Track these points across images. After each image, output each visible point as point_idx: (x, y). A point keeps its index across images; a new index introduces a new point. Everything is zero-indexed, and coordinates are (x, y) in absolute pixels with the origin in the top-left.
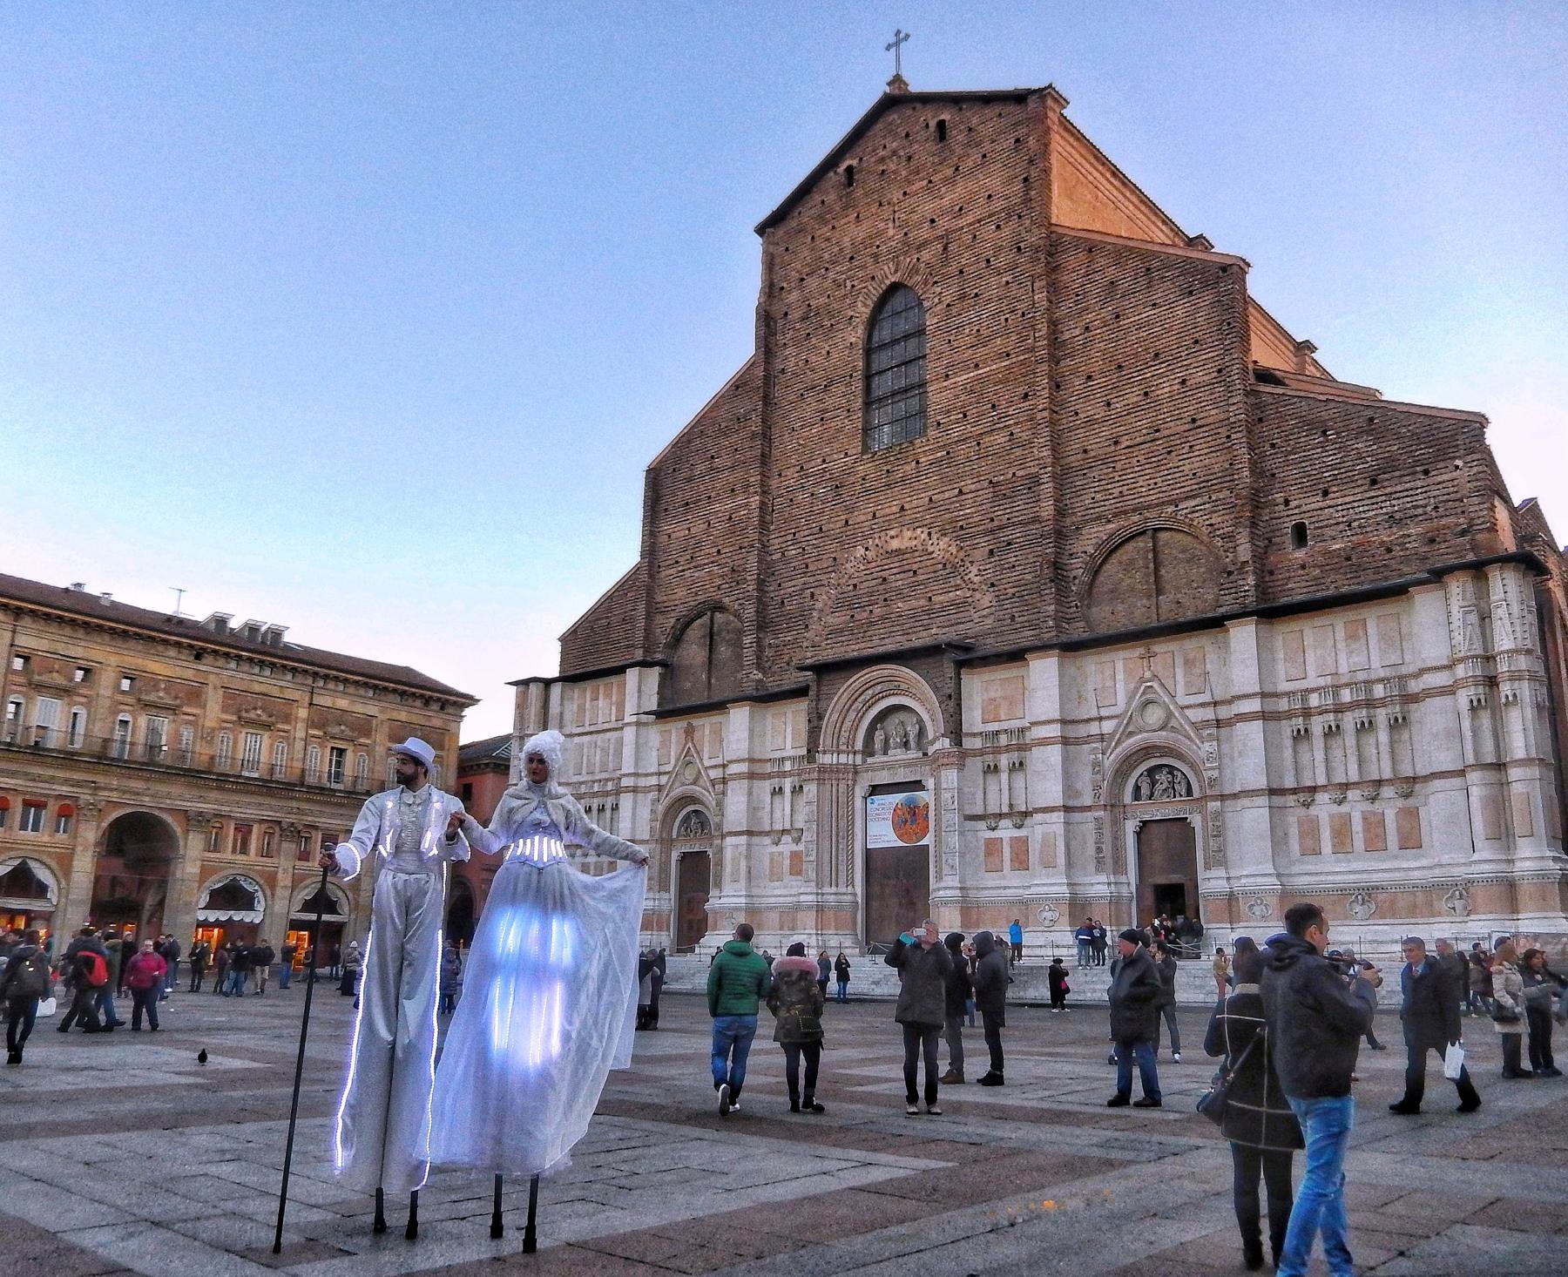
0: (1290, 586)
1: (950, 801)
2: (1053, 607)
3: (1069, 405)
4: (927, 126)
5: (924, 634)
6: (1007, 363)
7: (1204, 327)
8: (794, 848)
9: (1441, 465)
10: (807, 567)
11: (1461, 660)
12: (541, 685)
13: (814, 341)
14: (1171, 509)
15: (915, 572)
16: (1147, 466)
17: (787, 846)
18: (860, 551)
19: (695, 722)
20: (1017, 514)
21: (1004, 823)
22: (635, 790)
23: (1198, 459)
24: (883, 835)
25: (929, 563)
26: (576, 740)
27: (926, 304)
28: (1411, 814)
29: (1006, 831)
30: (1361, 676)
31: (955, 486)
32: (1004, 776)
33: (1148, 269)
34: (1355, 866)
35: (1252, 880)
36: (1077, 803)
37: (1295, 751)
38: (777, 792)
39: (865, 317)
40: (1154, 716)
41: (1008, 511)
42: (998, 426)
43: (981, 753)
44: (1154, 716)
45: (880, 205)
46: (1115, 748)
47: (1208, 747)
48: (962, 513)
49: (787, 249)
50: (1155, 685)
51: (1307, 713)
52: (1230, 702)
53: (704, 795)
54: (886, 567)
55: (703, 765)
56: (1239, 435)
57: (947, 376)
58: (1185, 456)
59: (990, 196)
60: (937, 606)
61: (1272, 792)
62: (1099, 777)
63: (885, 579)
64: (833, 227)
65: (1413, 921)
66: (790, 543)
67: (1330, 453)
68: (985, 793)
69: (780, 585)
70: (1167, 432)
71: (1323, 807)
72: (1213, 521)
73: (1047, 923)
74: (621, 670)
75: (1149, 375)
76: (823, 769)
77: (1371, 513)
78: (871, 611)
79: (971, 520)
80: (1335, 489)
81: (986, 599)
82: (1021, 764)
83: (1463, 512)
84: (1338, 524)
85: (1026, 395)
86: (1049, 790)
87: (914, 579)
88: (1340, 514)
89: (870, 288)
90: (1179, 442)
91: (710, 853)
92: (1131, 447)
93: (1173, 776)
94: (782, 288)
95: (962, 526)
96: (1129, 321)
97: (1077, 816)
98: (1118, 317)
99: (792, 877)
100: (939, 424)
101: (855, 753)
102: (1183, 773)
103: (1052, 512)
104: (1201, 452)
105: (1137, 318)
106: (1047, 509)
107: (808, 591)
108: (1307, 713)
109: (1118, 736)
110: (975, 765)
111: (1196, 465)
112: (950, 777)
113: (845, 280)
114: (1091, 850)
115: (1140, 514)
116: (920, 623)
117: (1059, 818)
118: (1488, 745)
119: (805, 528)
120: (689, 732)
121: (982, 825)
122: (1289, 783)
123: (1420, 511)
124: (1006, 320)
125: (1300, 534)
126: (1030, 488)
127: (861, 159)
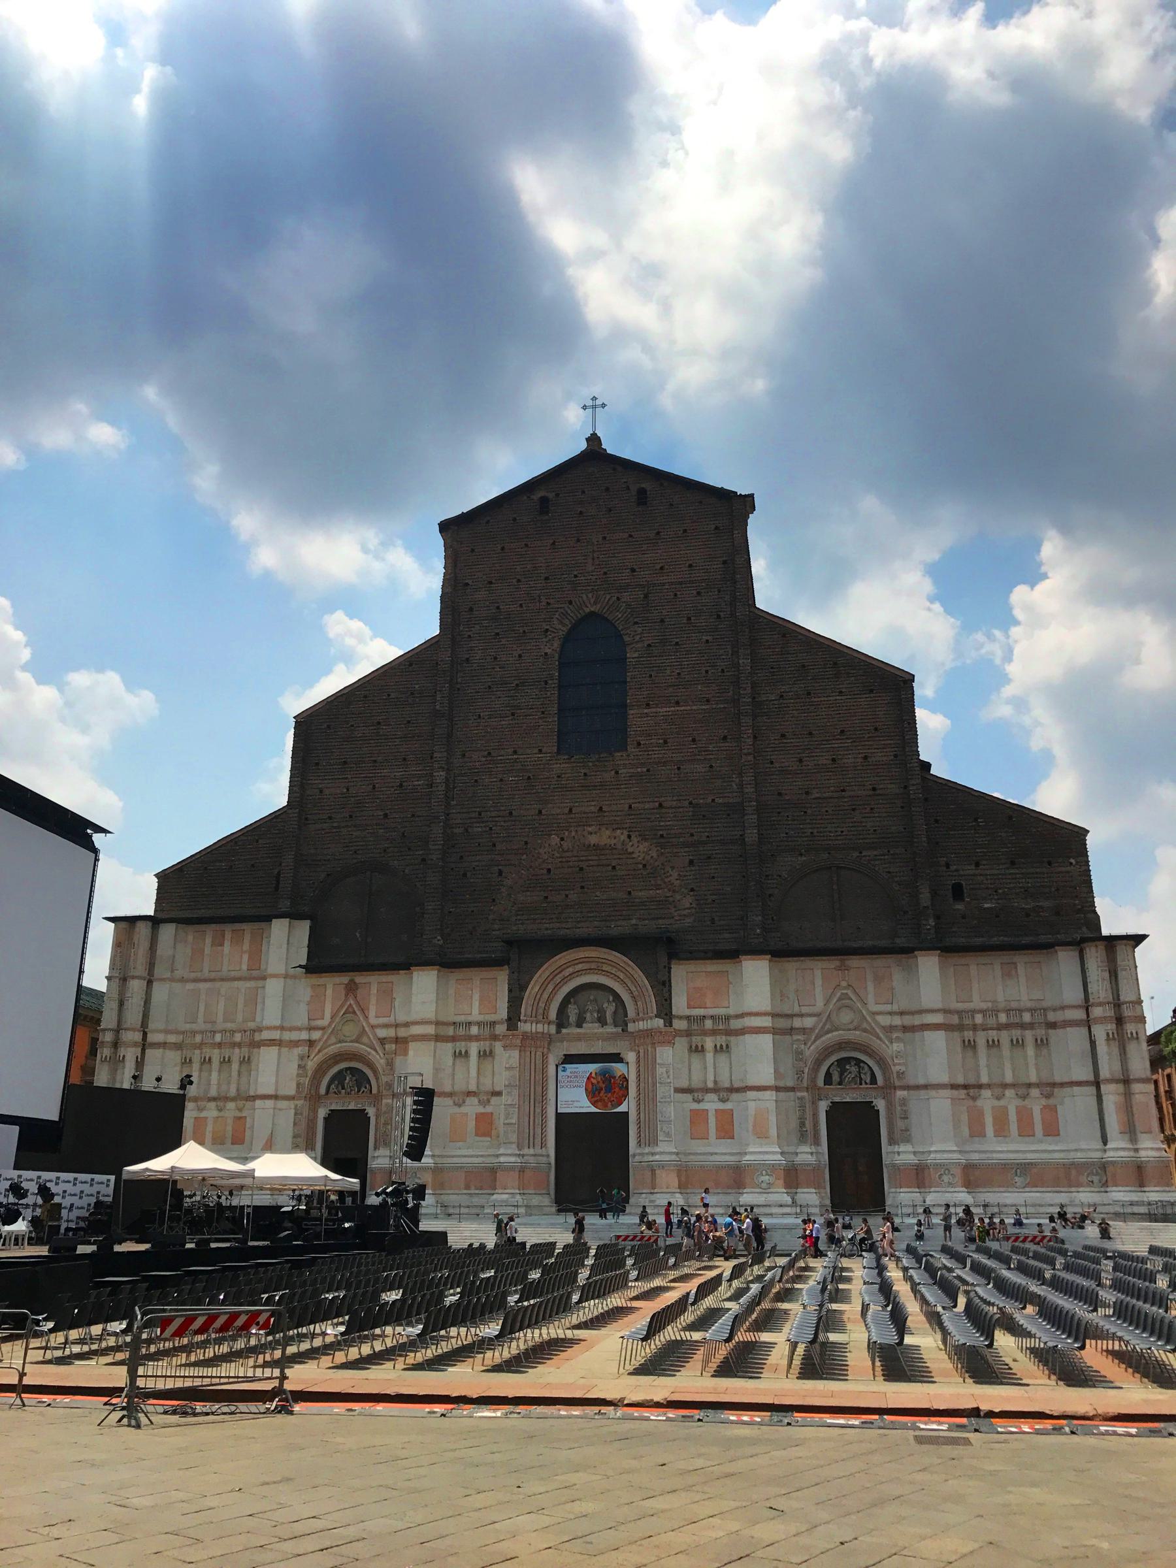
0: (954, 930)
1: (665, 1075)
2: (760, 918)
3: (766, 753)
4: (628, 488)
5: (624, 923)
6: (708, 707)
7: (883, 720)
8: (481, 1110)
9: (1060, 860)
10: (494, 845)
11: (1100, 1004)
12: (150, 924)
13: (504, 641)
14: (856, 854)
15: (614, 868)
16: (834, 817)
17: (472, 1108)
18: (555, 840)
19: (360, 979)
20: (716, 834)
21: (712, 1096)
22: (278, 1043)
23: (878, 819)
24: (577, 1101)
25: (630, 861)
26: (190, 986)
27: (626, 638)
28: (1053, 1109)
29: (711, 1104)
30: (1014, 1005)
31: (656, 800)
32: (709, 1056)
33: (835, 664)
34: (1012, 1147)
35: (938, 1156)
36: (781, 1084)
37: (964, 1058)
38: (462, 1055)
39: (561, 633)
40: (846, 1017)
41: (708, 830)
42: (699, 757)
43: (688, 1033)
44: (846, 1017)
45: (578, 540)
46: (815, 1041)
47: (896, 1047)
48: (662, 824)
49: (473, 551)
50: (850, 992)
51: (975, 1028)
52: (912, 1013)
53: (369, 1053)
54: (584, 858)
55: (368, 1023)
56: (918, 809)
57: (648, 705)
58: (867, 815)
59: (690, 566)
60: (637, 900)
61: (954, 1087)
62: (802, 1064)
63: (581, 869)
64: (526, 545)
65: (1058, 1189)
66: (475, 820)
67: (983, 835)
68: (690, 1070)
69: (461, 857)
70: (852, 793)
71: (986, 1101)
72: (891, 870)
73: (764, 1185)
74: (268, 919)
75: (836, 745)
76: (525, 1036)
77: (1012, 885)
78: (567, 896)
79: (672, 832)
80: (985, 862)
81: (687, 901)
82: (727, 1045)
83: (1077, 896)
84: (987, 888)
85: (725, 738)
86: (764, 1073)
87: (613, 874)
88: (989, 882)
89: (567, 609)
90: (861, 803)
91: (371, 1112)
92: (819, 798)
93: (859, 1067)
94: (467, 584)
95: (662, 836)
96: (819, 699)
97: (782, 1095)
98: (809, 694)
99: (478, 1138)
100: (639, 744)
101: (549, 1024)
102: (868, 1066)
103: (757, 839)
104: (881, 814)
105: (826, 699)
106: (752, 835)
107: (496, 868)
108: (975, 1028)
109: (817, 1031)
110: (681, 1043)
111: (878, 824)
112: (665, 1054)
113: (539, 596)
114: (794, 1123)
115: (829, 853)
116: (618, 913)
117: (772, 1096)
118: (1117, 1066)
119: (492, 809)
120: (351, 988)
121: (689, 1097)
122: (960, 1080)
123: (1047, 890)
124: (707, 672)
125: (958, 892)
126: (729, 815)
127: (557, 495)
